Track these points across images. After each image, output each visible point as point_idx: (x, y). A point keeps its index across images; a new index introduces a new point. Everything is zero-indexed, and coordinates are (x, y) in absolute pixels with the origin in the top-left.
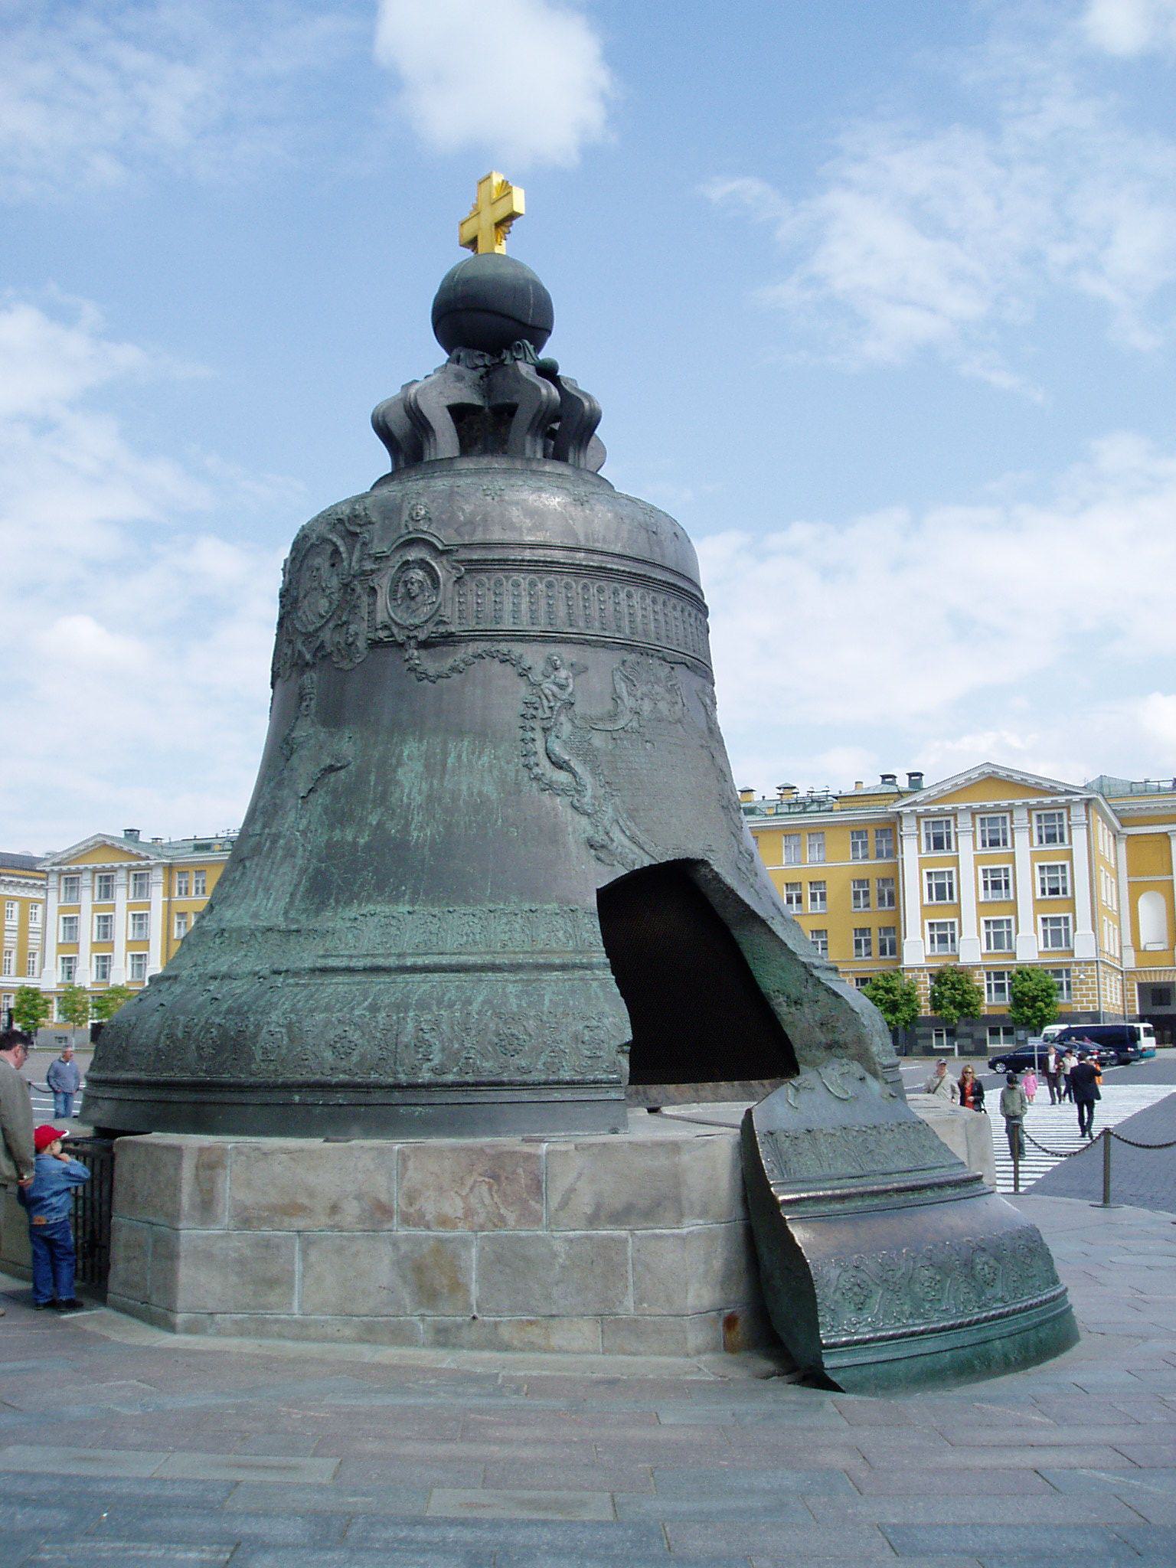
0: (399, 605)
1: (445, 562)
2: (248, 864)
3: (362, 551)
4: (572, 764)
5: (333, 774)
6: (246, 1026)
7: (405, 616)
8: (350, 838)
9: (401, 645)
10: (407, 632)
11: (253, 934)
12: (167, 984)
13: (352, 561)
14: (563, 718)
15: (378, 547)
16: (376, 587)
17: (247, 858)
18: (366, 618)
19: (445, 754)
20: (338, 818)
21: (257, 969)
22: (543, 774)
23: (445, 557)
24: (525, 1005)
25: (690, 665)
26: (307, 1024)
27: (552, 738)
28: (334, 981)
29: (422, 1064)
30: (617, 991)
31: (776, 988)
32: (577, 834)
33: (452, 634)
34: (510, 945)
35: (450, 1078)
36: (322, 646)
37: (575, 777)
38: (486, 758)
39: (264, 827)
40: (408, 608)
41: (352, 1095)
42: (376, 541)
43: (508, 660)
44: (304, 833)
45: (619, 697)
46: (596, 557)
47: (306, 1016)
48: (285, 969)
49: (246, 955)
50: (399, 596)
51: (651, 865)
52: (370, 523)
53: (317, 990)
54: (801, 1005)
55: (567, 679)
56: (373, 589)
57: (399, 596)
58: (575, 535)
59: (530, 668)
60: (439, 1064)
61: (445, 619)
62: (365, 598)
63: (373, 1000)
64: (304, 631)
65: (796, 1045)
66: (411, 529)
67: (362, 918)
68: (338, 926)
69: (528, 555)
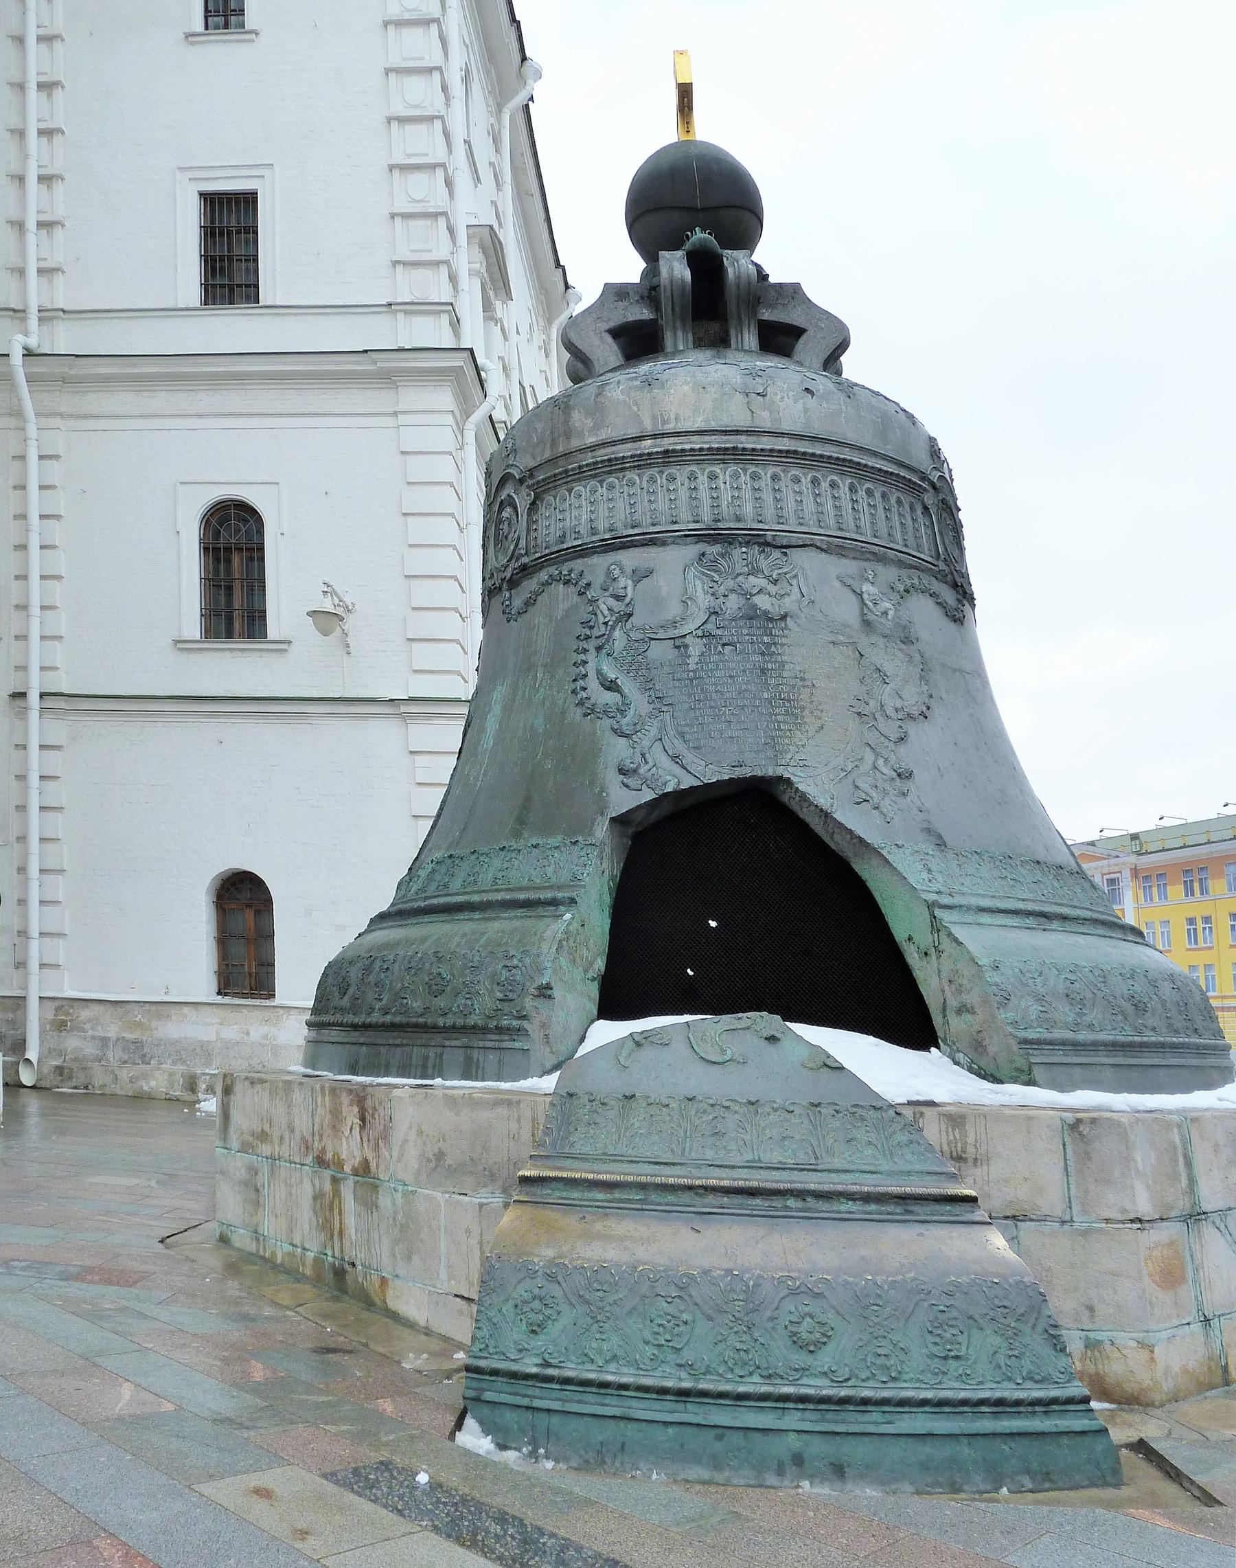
4: (619, 681)
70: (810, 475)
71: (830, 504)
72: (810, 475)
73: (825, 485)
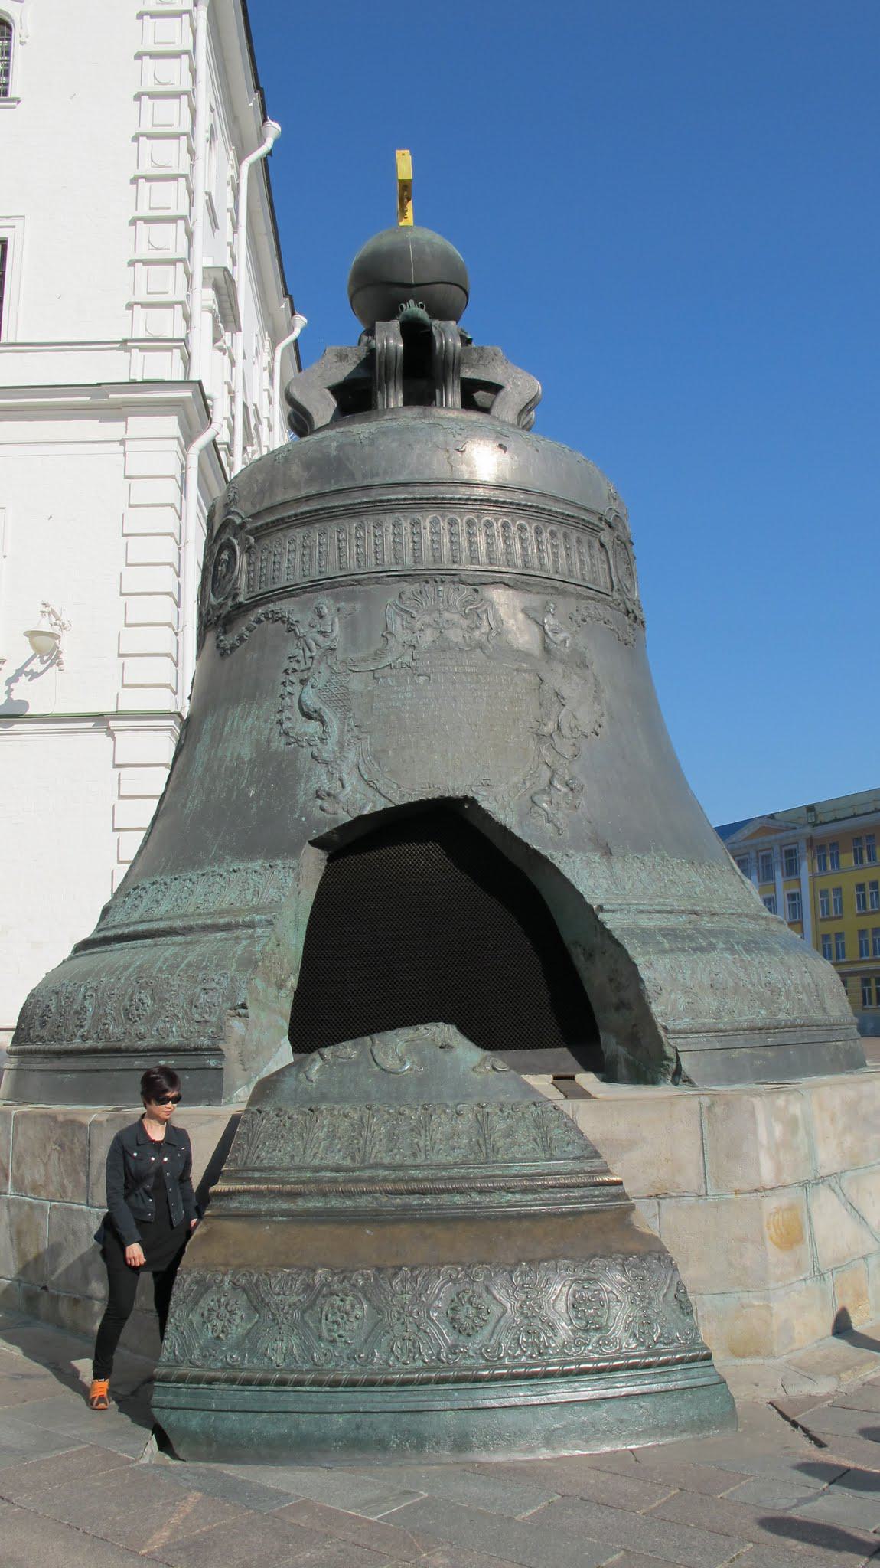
14: (323, 668)
19: (224, 725)
25: (511, 584)
35: (89, 1044)
43: (280, 618)
45: (390, 633)
46: (374, 492)
51: (385, 811)
58: (352, 476)
65: (595, 1006)
70: (500, 521)
71: (518, 547)
72: (500, 521)
73: (513, 529)
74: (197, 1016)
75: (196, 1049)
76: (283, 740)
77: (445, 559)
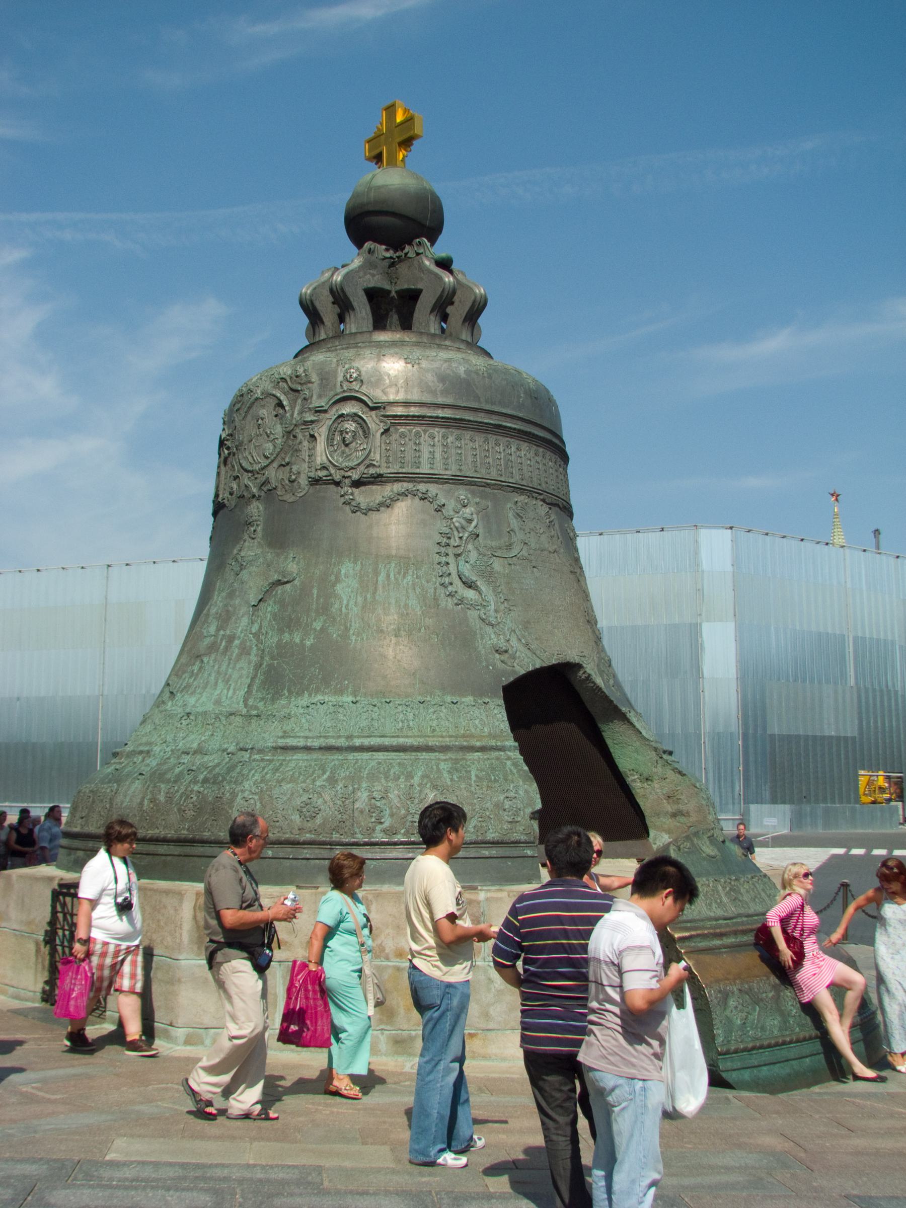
0: (336, 451)
1: (374, 417)
2: (205, 660)
3: (303, 406)
4: (478, 583)
5: (280, 587)
6: (223, 793)
7: (340, 459)
8: (297, 640)
9: (337, 484)
10: (342, 473)
11: (217, 718)
12: (140, 758)
13: (295, 413)
14: (470, 547)
15: (316, 403)
16: (316, 435)
17: (205, 655)
18: (307, 461)
19: (376, 573)
20: (287, 623)
21: (226, 746)
22: (456, 592)
23: (374, 412)
24: (456, 779)
26: (276, 792)
27: (461, 563)
28: (294, 758)
29: (375, 827)
30: (526, 768)
31: (631, 768)
32: (484, 641)
33: (380, 476)
34: (438, 729)
36: (267, 482)
37: (481, 594)
38: (409, 577)
39: (218, 630)
40: (343, 452)
41: (317, 851)
42: (315, 397)
43: (426, 498)
44: (256, 635)
47: (275, 786)
48: (250, 747)
49: (212, 735)
50: (335, 443)
52: (310, 382)
53: (281, 765)
54: (652, 781)
55: (472, 514)
56: (312, 436)
57: (335, 443)
59: (444, 505)
60: (389, 827)
61: (374, 463)
62: (305, 443)
63: (331, 773)
64: (250, 468)
66: (345, 388)
67: (313, 706)
68: (293, 712)
69: (440, 413)
74: (506, 817)
75: (513, 843)
76: (449, 600)
77: (535, 479)
